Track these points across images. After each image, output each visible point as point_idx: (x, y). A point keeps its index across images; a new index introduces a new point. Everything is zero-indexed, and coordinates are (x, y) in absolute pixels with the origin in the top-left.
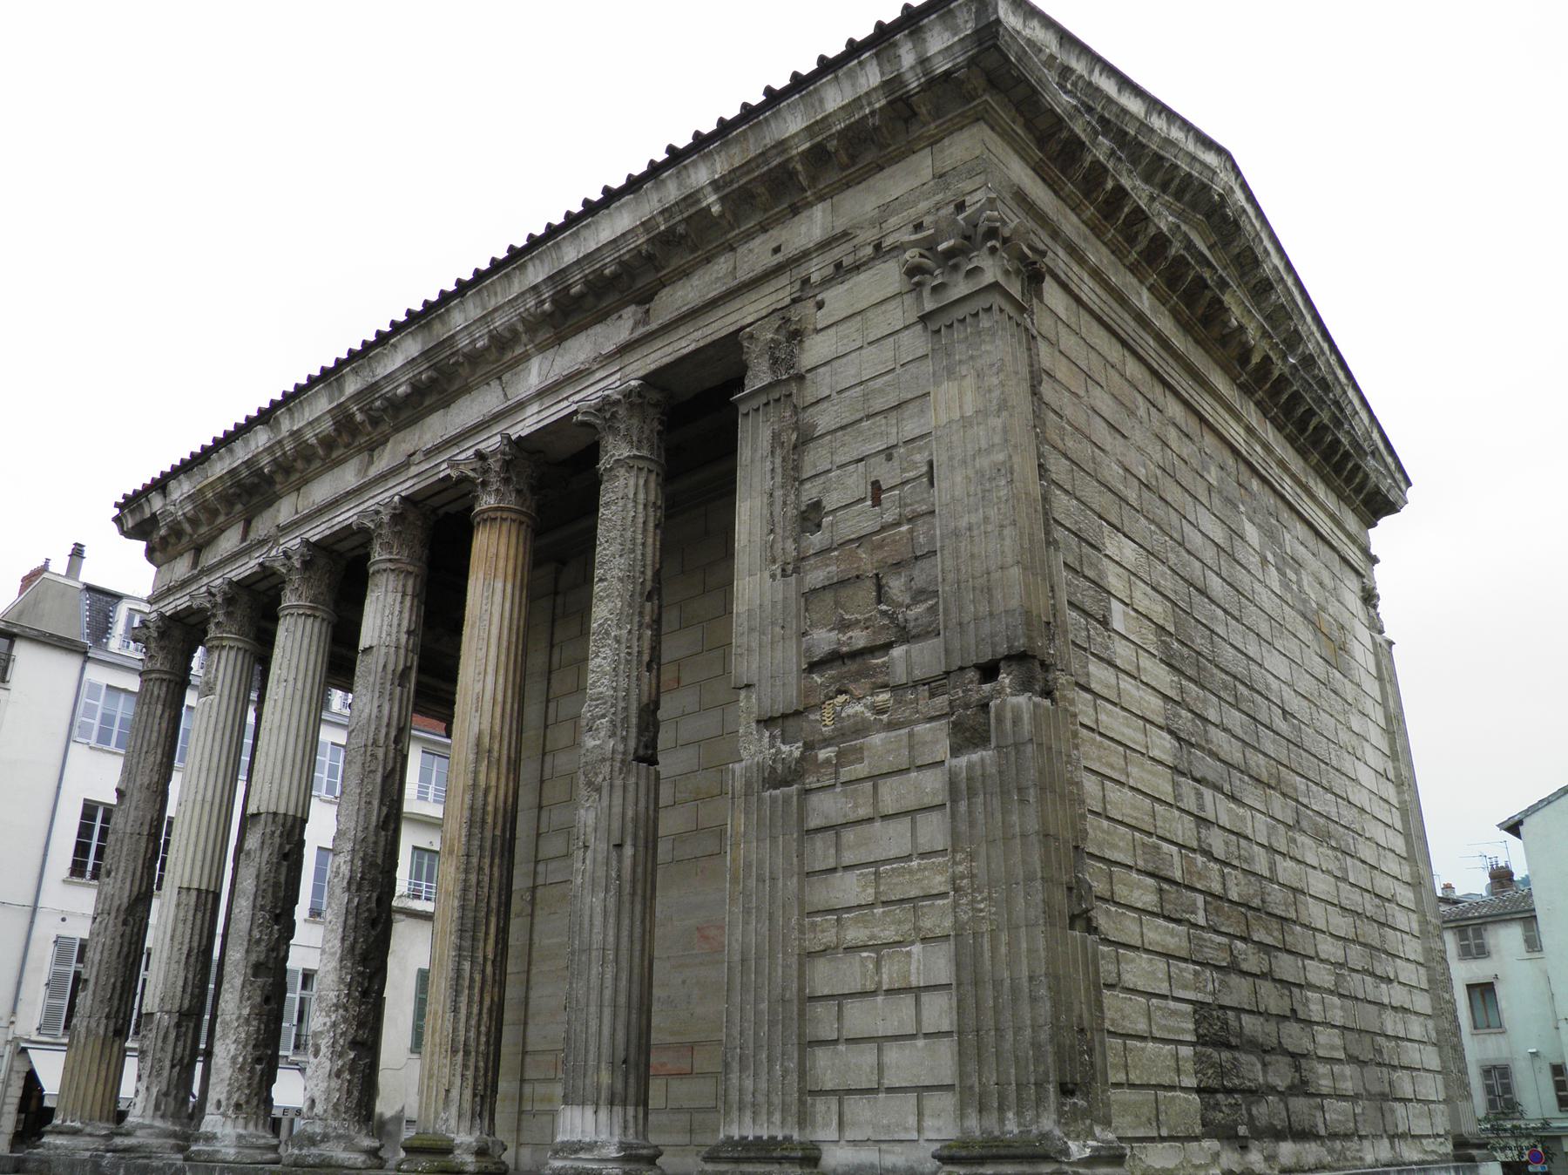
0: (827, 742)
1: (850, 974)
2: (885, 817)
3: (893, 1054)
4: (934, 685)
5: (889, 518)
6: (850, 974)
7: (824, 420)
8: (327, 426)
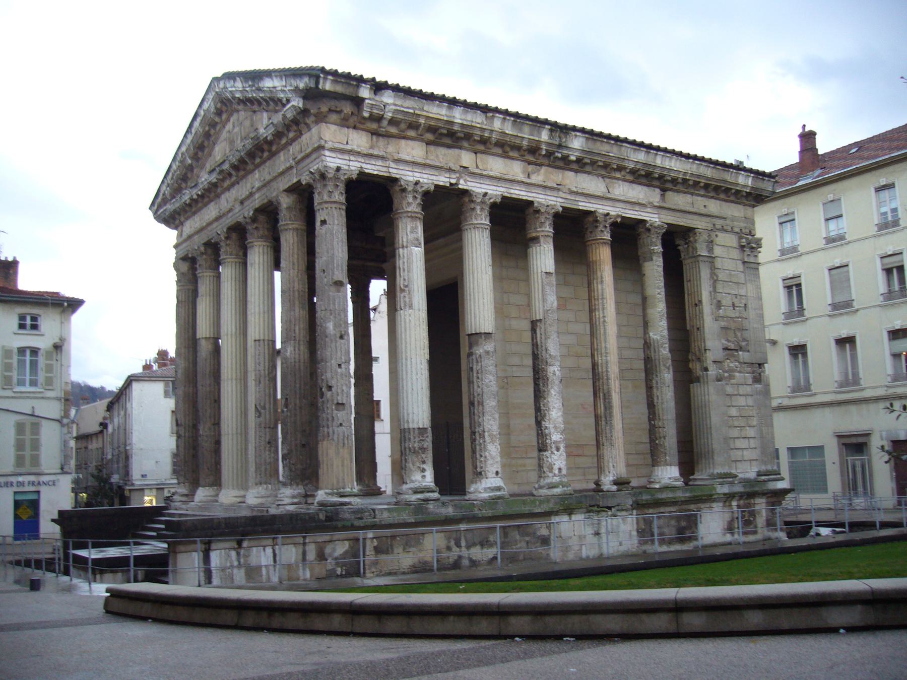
0: (726, 372)
1: (735, 433)
3: (745, 453)
5: (737, 315)
6: (735, 433)
7: (722, 276)
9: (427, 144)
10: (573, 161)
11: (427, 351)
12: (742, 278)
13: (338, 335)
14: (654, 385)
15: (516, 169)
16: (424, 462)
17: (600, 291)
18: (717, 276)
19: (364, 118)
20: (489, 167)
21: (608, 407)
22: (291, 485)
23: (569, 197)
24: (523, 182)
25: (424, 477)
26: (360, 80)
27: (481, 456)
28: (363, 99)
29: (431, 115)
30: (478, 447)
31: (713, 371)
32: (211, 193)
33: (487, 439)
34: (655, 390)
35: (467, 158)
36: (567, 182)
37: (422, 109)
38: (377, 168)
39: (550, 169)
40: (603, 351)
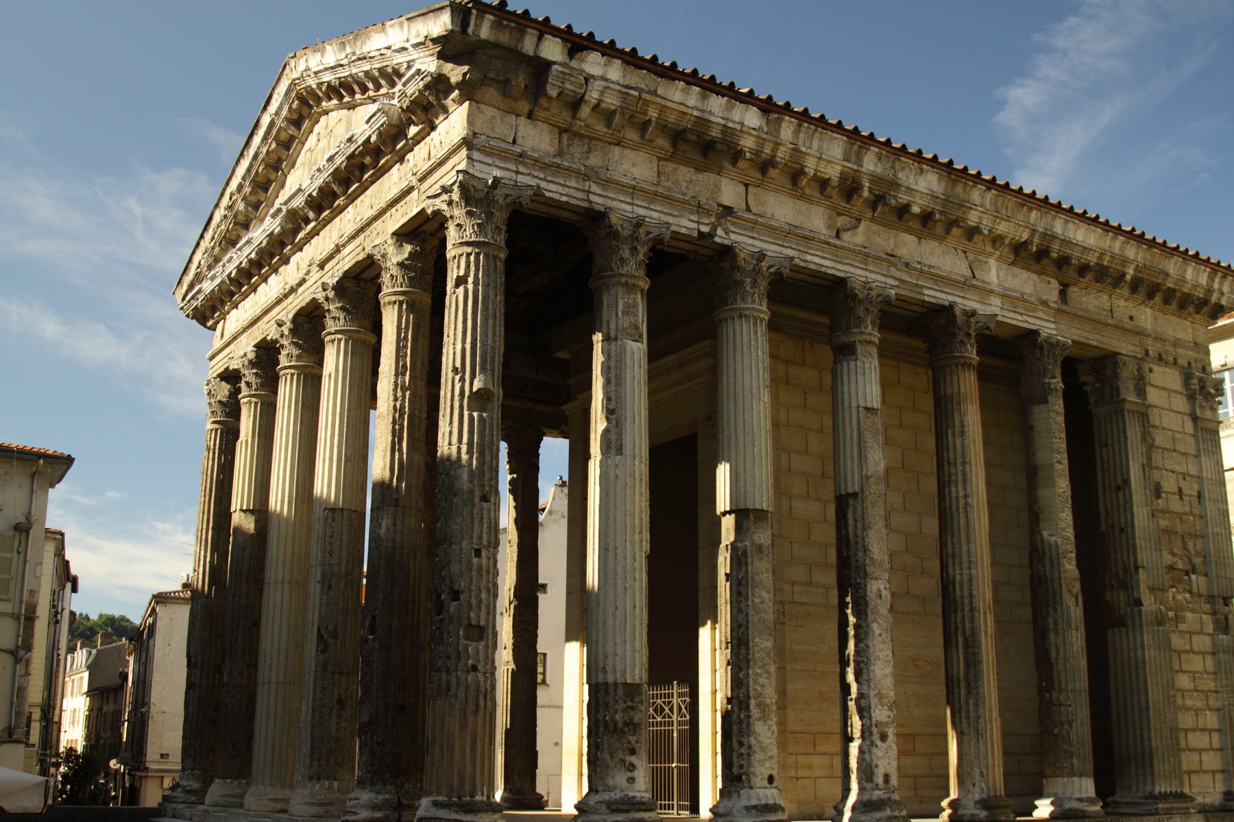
2: (1195, 653)
4: (1211, 598)
5: (1187, 509)
7: (1160, 439)
8: (833, 172)
9: (659, 159)
10: (914, 215)
11: (646, 536)
12: (1189, 445)
13: (477, 494)
14: (1051, 627)
15: (816, 219)
16: (633, 752)
17: (959, 450)
18: (1154, 440)
19: (550, 99)
20: (769, 213)
21: (973, 662)
22: (372, 783)
23: (907, 278)
24: (828, 243)
25: (632, 780)
26: (545, 28)
27: (741, 744)
28: (548, 64)
29: (669, 104)
30: (735, 727)
31: (1149, 603)
32: (274, 253)
33: (754, 711)
34: (1052, 636)
35: (730, 193)
36: (902, 252)
37: (655, 93)
38: (567, 191)
39: (875, 227)
40: (965, 558)
